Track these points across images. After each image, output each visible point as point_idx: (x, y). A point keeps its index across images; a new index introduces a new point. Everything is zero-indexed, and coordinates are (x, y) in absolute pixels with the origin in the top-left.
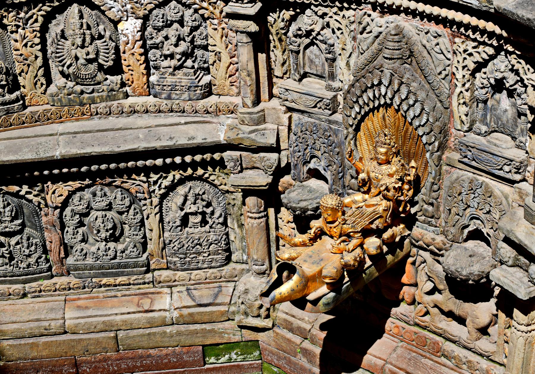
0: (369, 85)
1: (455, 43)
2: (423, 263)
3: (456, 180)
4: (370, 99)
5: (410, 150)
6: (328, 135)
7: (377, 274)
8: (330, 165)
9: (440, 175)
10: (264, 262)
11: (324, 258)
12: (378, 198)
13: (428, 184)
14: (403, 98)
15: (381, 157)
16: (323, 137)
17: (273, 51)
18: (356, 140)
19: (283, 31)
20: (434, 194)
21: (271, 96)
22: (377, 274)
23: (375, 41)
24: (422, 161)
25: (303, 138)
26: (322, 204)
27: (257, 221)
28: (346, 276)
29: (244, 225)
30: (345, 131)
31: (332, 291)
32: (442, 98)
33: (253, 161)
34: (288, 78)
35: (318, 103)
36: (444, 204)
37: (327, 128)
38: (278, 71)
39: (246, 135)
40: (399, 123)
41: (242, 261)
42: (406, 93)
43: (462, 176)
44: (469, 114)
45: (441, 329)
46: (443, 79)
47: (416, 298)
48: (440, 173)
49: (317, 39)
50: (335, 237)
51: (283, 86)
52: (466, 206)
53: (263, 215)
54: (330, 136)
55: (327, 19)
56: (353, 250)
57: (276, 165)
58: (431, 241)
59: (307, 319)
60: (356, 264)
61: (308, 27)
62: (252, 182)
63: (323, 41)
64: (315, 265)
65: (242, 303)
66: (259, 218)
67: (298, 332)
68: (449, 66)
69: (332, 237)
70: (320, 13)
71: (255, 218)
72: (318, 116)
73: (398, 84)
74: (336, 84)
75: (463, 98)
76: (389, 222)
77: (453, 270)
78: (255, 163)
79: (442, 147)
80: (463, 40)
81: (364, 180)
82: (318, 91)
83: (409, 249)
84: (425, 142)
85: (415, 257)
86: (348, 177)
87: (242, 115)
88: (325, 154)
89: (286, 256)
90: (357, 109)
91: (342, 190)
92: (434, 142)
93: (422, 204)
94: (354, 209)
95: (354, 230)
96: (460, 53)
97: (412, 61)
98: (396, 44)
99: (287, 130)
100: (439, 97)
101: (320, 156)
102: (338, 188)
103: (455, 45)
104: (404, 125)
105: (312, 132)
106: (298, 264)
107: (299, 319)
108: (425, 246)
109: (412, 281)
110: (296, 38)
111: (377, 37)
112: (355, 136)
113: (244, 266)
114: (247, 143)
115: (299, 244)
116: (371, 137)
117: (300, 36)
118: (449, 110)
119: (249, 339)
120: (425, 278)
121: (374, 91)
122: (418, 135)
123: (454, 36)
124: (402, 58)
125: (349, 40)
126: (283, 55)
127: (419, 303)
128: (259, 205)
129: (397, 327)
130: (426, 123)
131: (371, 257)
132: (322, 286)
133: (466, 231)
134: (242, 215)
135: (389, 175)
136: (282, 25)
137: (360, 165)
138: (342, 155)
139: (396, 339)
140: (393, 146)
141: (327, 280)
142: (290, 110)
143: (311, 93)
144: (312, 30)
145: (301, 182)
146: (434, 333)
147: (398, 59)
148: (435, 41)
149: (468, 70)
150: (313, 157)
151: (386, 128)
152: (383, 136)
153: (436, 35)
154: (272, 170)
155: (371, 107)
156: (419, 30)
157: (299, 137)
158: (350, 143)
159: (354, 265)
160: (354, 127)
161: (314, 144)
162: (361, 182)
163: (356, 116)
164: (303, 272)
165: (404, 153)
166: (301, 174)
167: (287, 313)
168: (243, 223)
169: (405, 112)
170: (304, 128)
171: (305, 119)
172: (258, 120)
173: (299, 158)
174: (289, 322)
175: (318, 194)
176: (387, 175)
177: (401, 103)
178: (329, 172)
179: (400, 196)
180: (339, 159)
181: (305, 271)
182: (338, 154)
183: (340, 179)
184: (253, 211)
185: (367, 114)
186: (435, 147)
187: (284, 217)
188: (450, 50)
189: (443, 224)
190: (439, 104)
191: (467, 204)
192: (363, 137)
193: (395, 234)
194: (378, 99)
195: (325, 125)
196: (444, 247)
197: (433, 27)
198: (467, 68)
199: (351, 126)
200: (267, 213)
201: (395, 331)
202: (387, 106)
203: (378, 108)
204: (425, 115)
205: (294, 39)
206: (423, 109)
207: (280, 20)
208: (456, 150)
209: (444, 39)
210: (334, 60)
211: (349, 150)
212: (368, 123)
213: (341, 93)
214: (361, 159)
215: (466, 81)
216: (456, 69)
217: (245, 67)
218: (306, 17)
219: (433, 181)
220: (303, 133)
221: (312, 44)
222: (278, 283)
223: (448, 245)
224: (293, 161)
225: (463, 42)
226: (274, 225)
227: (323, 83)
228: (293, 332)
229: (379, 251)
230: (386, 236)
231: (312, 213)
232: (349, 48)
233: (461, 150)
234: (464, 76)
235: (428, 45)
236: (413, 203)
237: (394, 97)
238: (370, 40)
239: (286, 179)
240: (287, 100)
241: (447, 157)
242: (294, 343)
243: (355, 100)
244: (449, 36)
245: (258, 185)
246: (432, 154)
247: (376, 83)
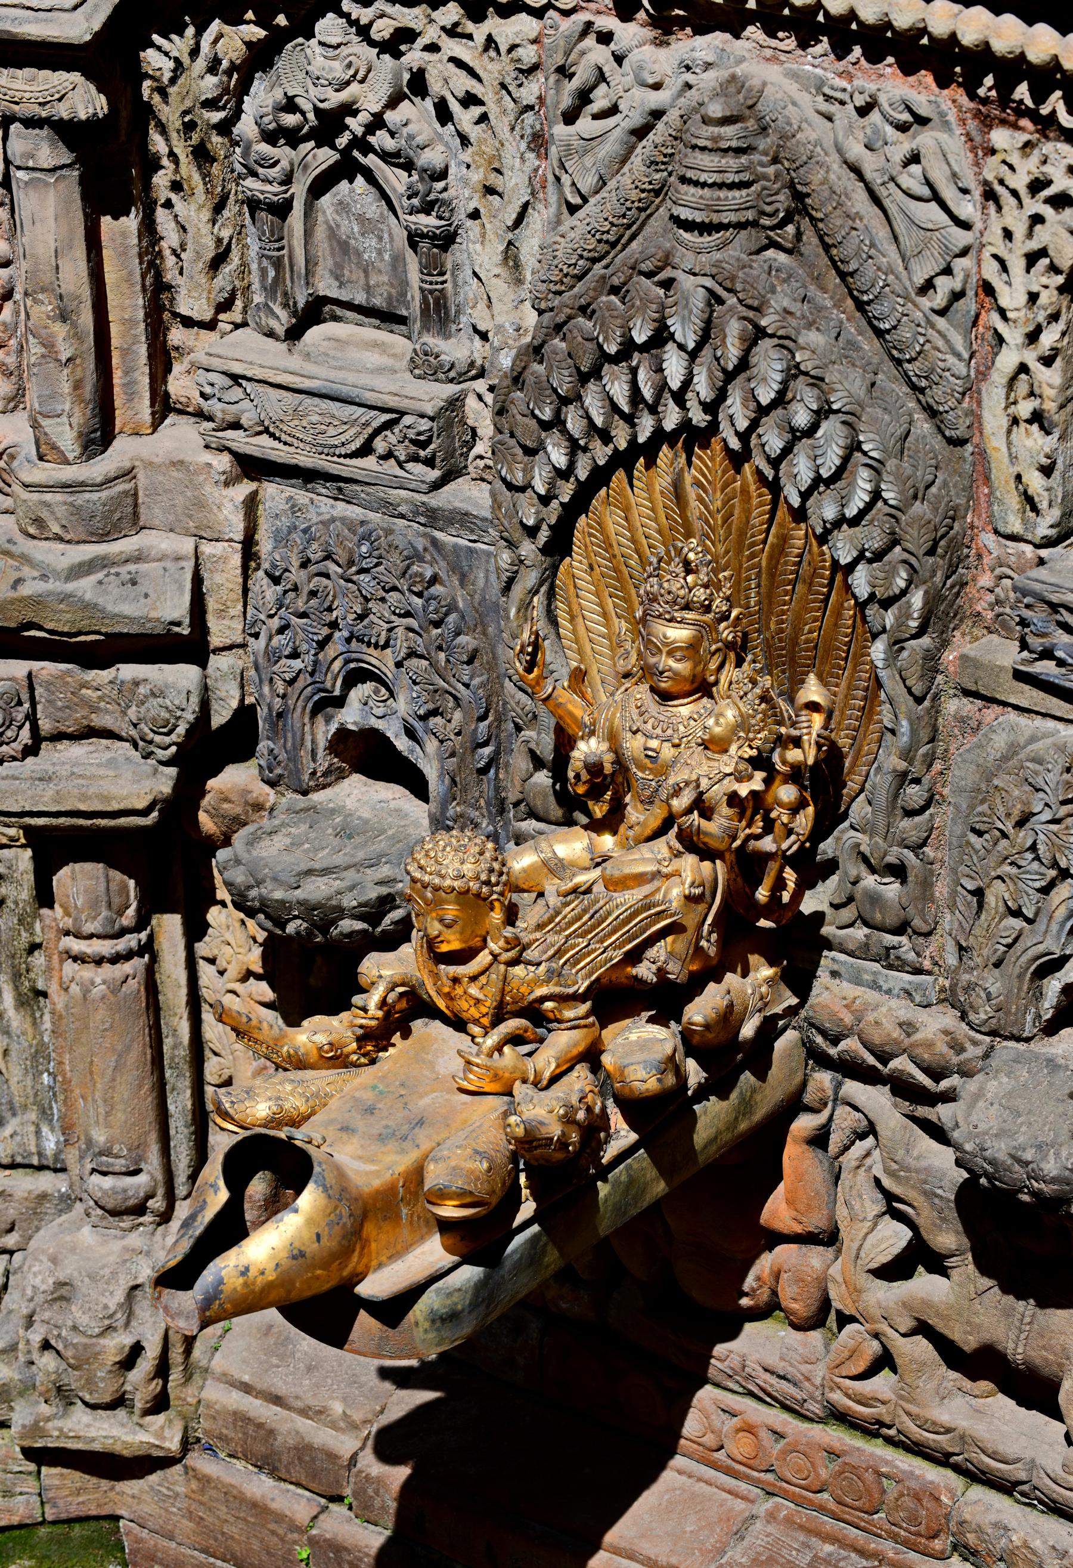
0: (612, 349)
1: (993, 152)
2: (862, 1136)
3: (1005, 758)
4: (615, 408)
5: (797, 631)
6: (428, 574)
7: (660, 1187)
8: (434, 713)
9: (932, 740)
10: (140, 1159)
11: (428, 1113)
12: (661, 847)
13: (881, 782)
14: (765, 400)
15: (671, 663)
16: (403, 585)
17: (168, 204)
18: (551, 595)
19: (216, 117)
20: (906, 823)
21: (164, 407)
22: (660, 1187)
23: (631, 150)
24: (852, 677)
25: (313, 594)
26: (417, 875)
27: (108, 971)
28: (525, 1192)
29: (44, 994)
30: (506, 557)
31: (467, 1259)
32: (936, 395)
33: (86, 703)
34: (237, 326)
35: (377, 432)
36: (954, 871)
37: (420, 544)
38: (193, 301)
39: (53, 585)
40: (747, 513)
41: (35, 1161)
42: (779, 377)
43: (1033, 739)
44: (1060, 466)
45: (948, 1431)
46: (942, 312)
47: (832, 1295)
48: (935, 729)
49: (367, 149)
50: (476, 1022)
51: (216, 363)
52: (1053, 873)
53: (134, 944)
54: (434, 580)
55: (414, 56)
56: (555, 1079)
57: (191, 717)
58: (897, 1033)
59: (337, 1408)
60: (574, 1137)
61: (329, 93)
62: (84, 798)
63: (397, 154)
64: (392, 1145)
65: (46, 1345)
66: (116, 959)
67: (298, 1473)
68: (964, 252)
69: (459, 1024)
70: (382, 30)
71: (99, 961)
72: (380, 492)
73: (742, 339)
74: (458, 349)
75: (1032, 394)
76: (712, 951)
77: (1002, 1156)
78: (95, 710)
79: (940, 618)
80: (1026, 137)
81: (594, 768)
82: (380, 382)
83: (798, 1078)
84: (862, 591)
85: (826, 1113)
86: (521, 763)
87: (35, 497)
88: (414, 662)
89: (262, 1110)
90: (558, 457)
91: (492, 822)
92: (904, 592)
93: (853, 872)
94: (553, 900)
95: (558, 990)
96: (1015, 193)
97: (799, 235)
98: (731, 162)
99: (236, 560)
100: (922, 391)
101: (389, 670)
102: (474, 814)
103: (993, 161)
104: (770, 522)
105: (351, 563)
106: (317, 1139)
107: (304, 1412)
108: (871, 1060)
109: (815, 1222)
110: (273, 143)
111: (640, 133)
112: (549, 581)
113: (46, 1182)
114: (59, 621)
115: (314, 1057)
116: (619, 579)
117: (293, 137)
118: (969, 448)
119: (75, 1511)
120: (874, 1205)
121: (634, 371)
122: (835, 562)
123: (987, 123)
124: (754, 224)
125: (514, 149)
126: (214, 222)
127: (844, 1320)
128: (117, 901)
129: (749, 1429)
130: (869, 506)
131: (635, 1109)
132: (422, 1239)
133: (1053, 986)
134: (34, 947)
135: (705, 745)
136: (209, 86)
137: (574, 705)
138: (492, 666)
139: (743, 1487)
140: (725, 617)
141: (449, 1211)
142: (252, 467)
143: (344, 391)
144: (350, 109)
145: (305, 793)
146: (916, 1449)
147: (740, 226)
148: (903, 145)
149: (1054, 269)
150: (356, 676)
151: (688, 535)
152: (680, 569)
153: (906, 117)
154: (174, 737)
155: (622, 445)
156: (828, 98)
157: (295, 588)
158: (526, 606)
159: (563, 1144)
160: (544, 535)
161: (361, 617)
162: (585, 776)
163: (552, 485)
164: (340, 1173)
165: (768, 646)
166: (304, 754)
167: (247, 1388)
168: (40, 985)
169: (775, 463)
170: (315, 546)
171: (321, 506)
172: (107, 516)
173: (291, 682)
174: (260, 1426)
175: (381, 845)
176: (697, 746)
177: (754, 424)
178: (431, 745)
179: (758, 837)
180: (476, 681)
181: (350, 1173)
182: (470, 662)
183: (483, 771)
184: (89, 928)
185: (600, 476)
186: (909, 616)
187: (225, 955)
188: (969, 180)
189: (952, 960)
190: (923, 426)
191: (1055, 864)
192: (584, 581)
193: (737, 1008)
194: (653, 410)
195: (409, 533)
196: (955, 1060)
197: (891, 85)
198: (1045, 261)
199: (532, 532)
200: (151, 938)
201: (740, 1447)
202: (693, 438)
203: (649, 451)
204: (865, 473)
205: (264, 148)
206: (854, 447)
207: (201, 64)
208: (1004, 626)
209: (943, 137)
210: (447, 240)
211: (526, 635)
212: (606, 516)
213: (481, 385)
214: (579, 677)
215: (1041, 317)
216: (995, 265)
217: (48, 277)
218: (319, 50)
219: (902, 765)
220: (313, 569)
221: (346, 168)
222: (228, 1230)
223: (972, 1052)
224: (267, 699)
225: (1027, 145)
226: (184, 991)
227: (396, 341)
228: (274, 1473)
229: (670, 1080)
230: (700, 1010)
231: (359, 925)
232: (515, 183)
233: (1023, 623)
234: (1033, 297)
235: (870, 164)
236: (812, 869)
237: (722, 395)
238: (610, 148)
239: (235, 779)
240: (236, 426)
241: (964, 658)
242: (280, 1518)
243: (547, 414)
244: (963, 122)
245: (115, 806)
246: (897, 644)
247: (640, 337)
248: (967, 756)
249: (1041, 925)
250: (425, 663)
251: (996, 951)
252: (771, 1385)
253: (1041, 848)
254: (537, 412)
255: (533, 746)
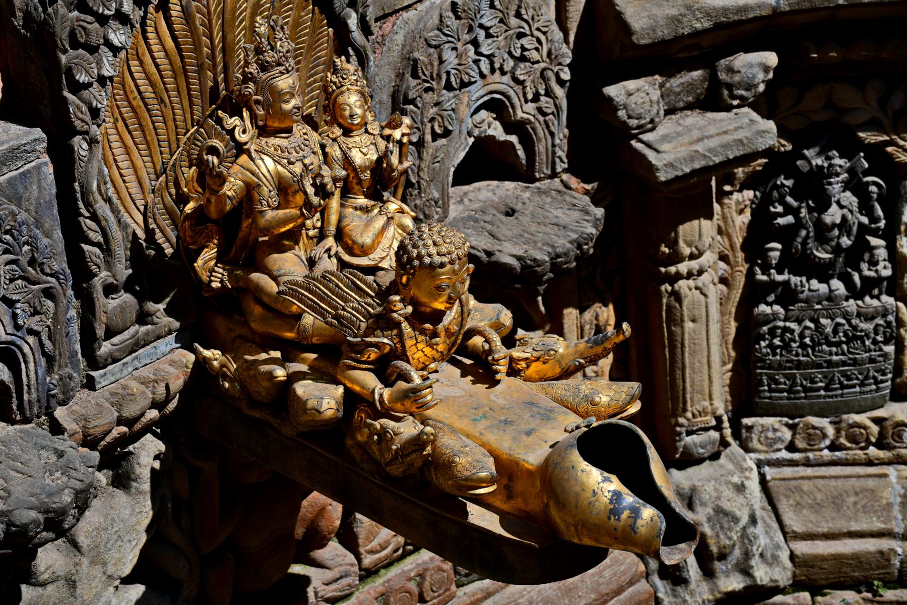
90: (118, 36)
183: (67, 335)
248: (382, 62)
249: (456, 133)
250: (20, 282)
251: (434, 169)
252: (335, 590)
253: (453, 79)
254: (107, 12)
255: (111, 280)
